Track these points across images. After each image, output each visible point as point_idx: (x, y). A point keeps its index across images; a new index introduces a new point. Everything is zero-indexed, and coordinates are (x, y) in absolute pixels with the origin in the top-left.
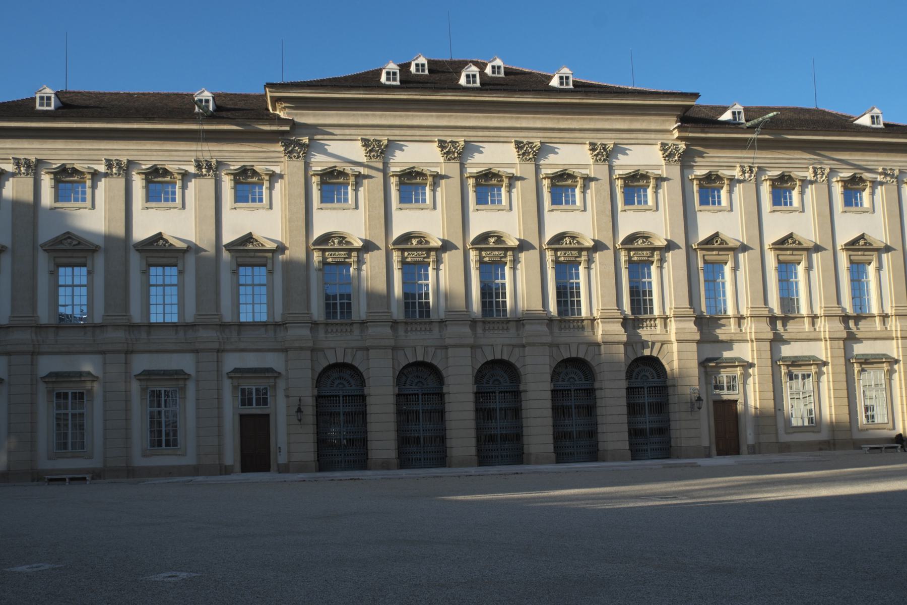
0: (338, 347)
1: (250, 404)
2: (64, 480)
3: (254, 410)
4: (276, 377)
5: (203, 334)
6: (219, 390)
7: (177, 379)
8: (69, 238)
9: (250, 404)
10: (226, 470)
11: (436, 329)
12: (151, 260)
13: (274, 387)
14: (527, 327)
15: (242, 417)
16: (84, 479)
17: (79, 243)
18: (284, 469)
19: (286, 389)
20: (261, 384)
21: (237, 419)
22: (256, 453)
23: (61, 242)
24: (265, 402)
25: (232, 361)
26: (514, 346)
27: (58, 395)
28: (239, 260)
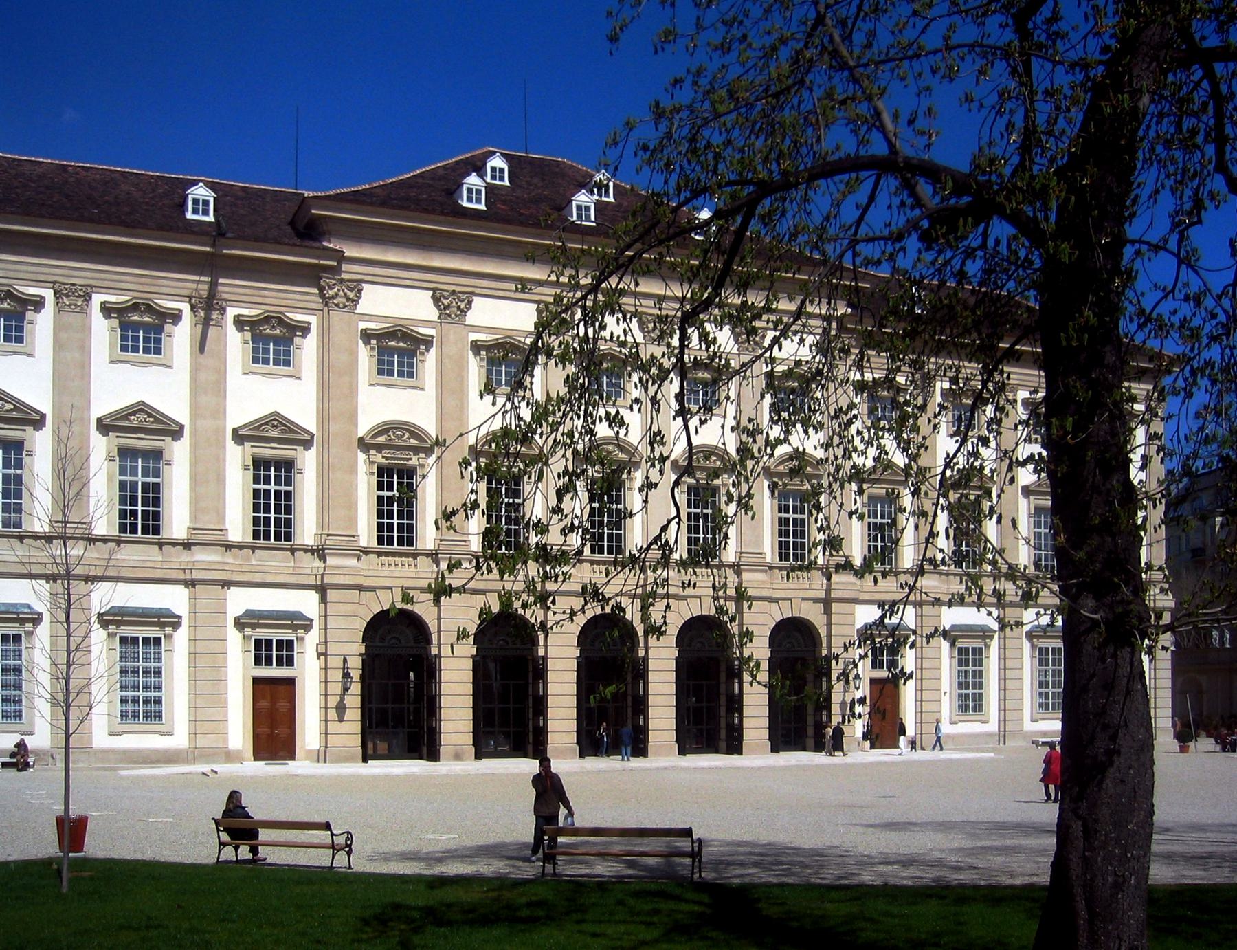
3: (274, 671)
5: (201, 556)
8: (141, 411)
15: (257, 681)
17: (16, 408)
20: (286, 635)
24: (290, 662)
27: (123, 640)
28: (256, 450)
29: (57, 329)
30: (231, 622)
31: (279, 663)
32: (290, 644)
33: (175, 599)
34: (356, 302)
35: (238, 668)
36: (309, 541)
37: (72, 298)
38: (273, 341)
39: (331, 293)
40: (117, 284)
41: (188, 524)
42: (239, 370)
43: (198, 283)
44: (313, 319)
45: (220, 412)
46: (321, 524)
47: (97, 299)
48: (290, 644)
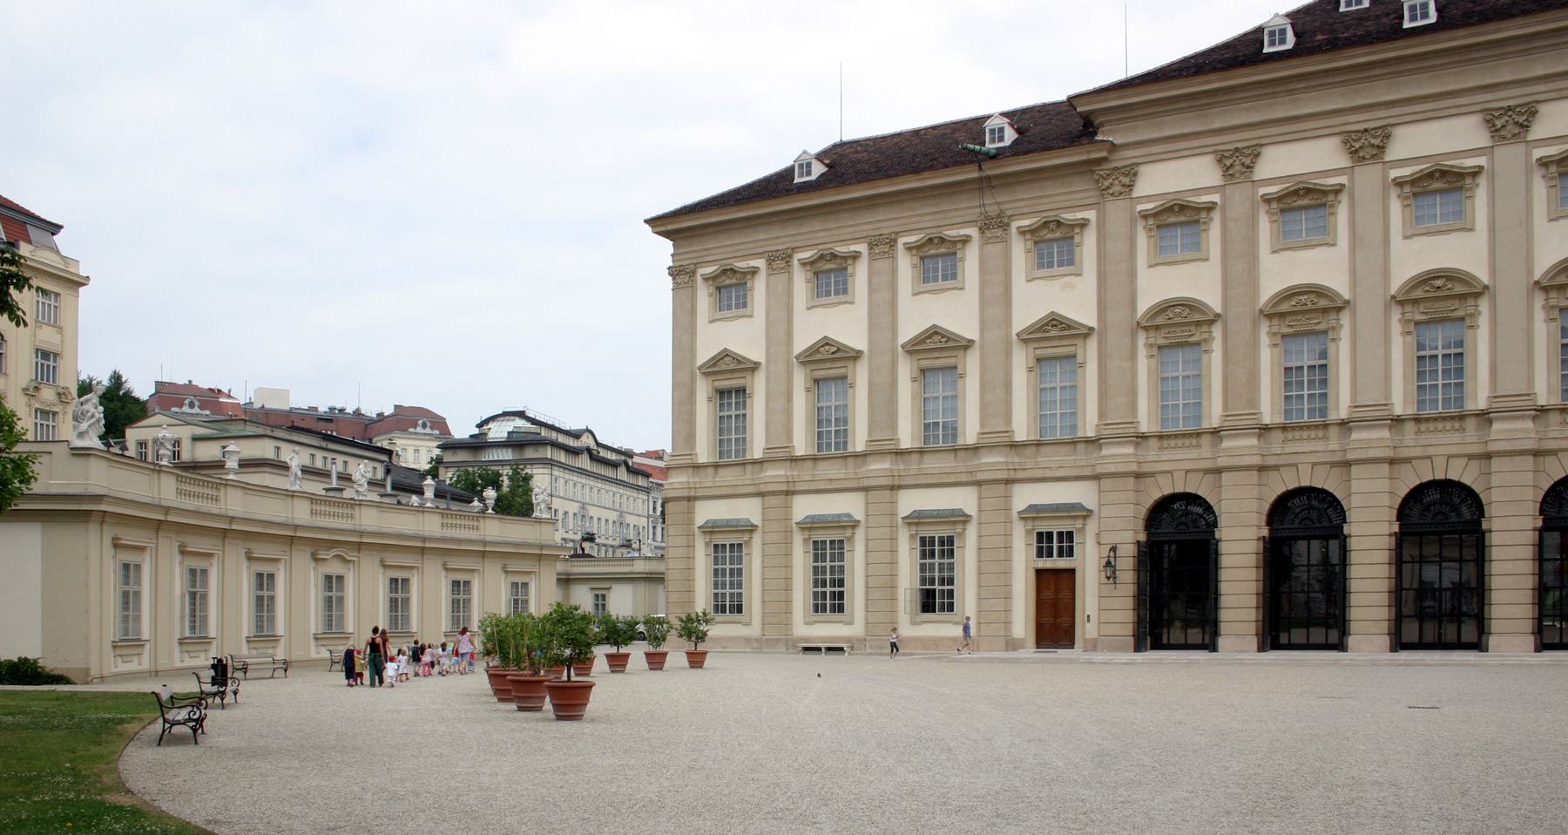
0: (1176, 471)
1: (1050, 555)
2: (819, 649)
4: (1085, 517)
5: (989, 459)
6: (1008, 535)
7: (955, 523)
9: (1050, 555)
10: (1012, 644)
11: (1333, 432)
12: (925, 364)
13: (1082, 530)
14: (1496, 426)
15: (1039, 572)
16: (841, 649)
18: (1093, 646)
19: (1098, 534)
20: (1065, 526)
21: (1032, 575)
22: (1055, 623)
23: (817, 351)
24: (1070, 553)
25: (1025, 496)
26: (1471, 457)
28: (1039, 352)
29: (871, 275)
30: (1015, 515)
31: (1060, 554)
32: (1070, 535)
33: (963, 499)
34: (1130, 187)
35: (1023, 563)
36: (1091, 433)
37: (883, 246)
38: (1054, 243)
39: (1106, 183)
40: (911, 226)
41: (978, 430)
42: (1023, 276)
43: (968, 206)
44: (1091, 215)
45: (1008, 320)
46: (1102, 415)
47: (901, 241)
48: (1070, 535)
